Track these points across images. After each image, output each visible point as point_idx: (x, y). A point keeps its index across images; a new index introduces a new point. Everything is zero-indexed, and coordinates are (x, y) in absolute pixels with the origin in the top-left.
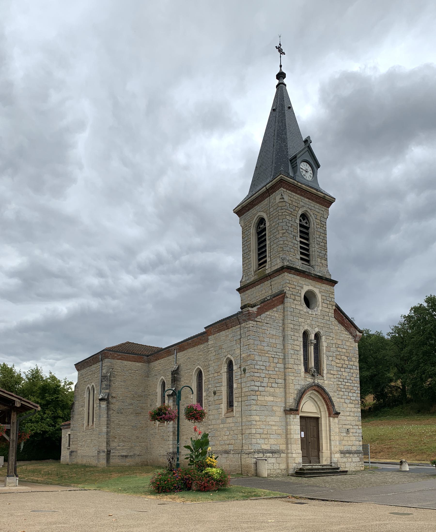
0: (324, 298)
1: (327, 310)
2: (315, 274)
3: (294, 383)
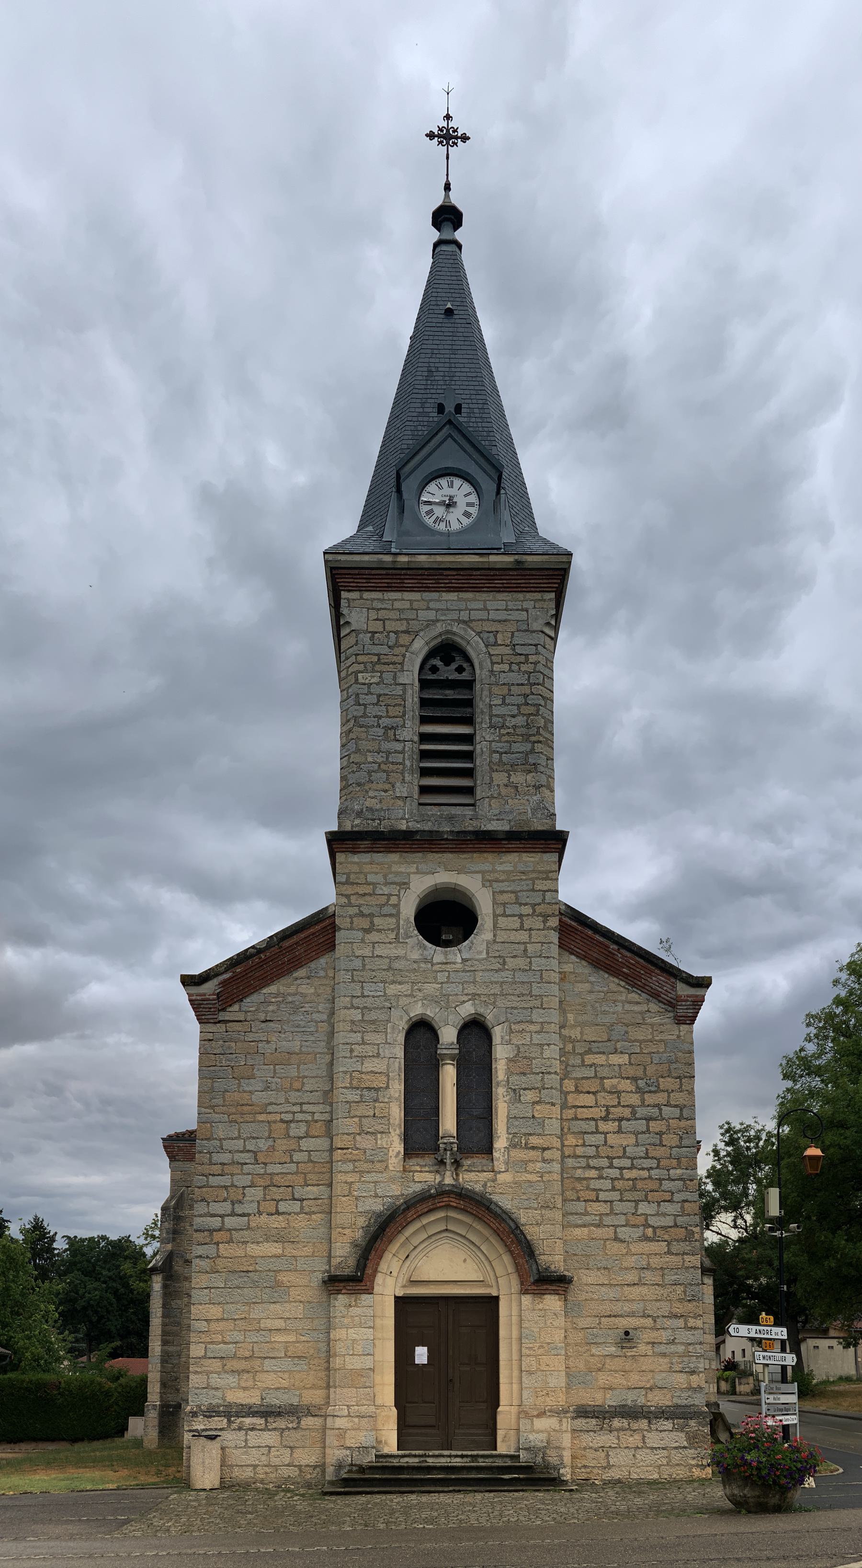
0: (505, 897)
1: (523, 936)
2: (458, 832)
3: (355, 1193)
